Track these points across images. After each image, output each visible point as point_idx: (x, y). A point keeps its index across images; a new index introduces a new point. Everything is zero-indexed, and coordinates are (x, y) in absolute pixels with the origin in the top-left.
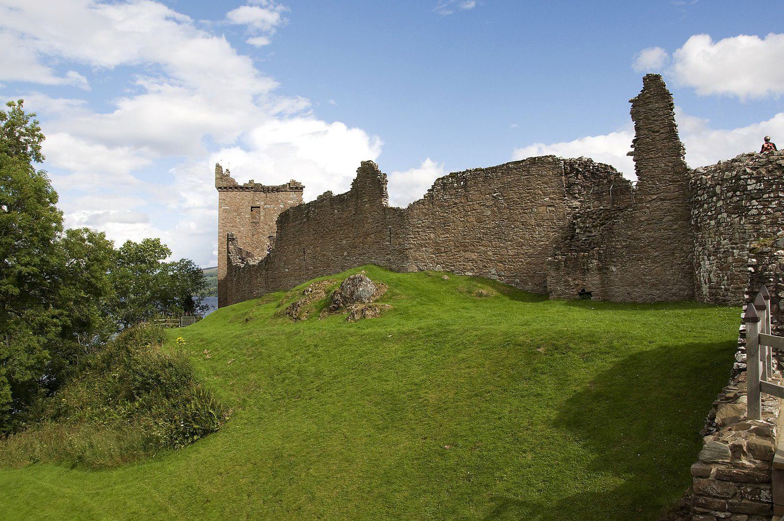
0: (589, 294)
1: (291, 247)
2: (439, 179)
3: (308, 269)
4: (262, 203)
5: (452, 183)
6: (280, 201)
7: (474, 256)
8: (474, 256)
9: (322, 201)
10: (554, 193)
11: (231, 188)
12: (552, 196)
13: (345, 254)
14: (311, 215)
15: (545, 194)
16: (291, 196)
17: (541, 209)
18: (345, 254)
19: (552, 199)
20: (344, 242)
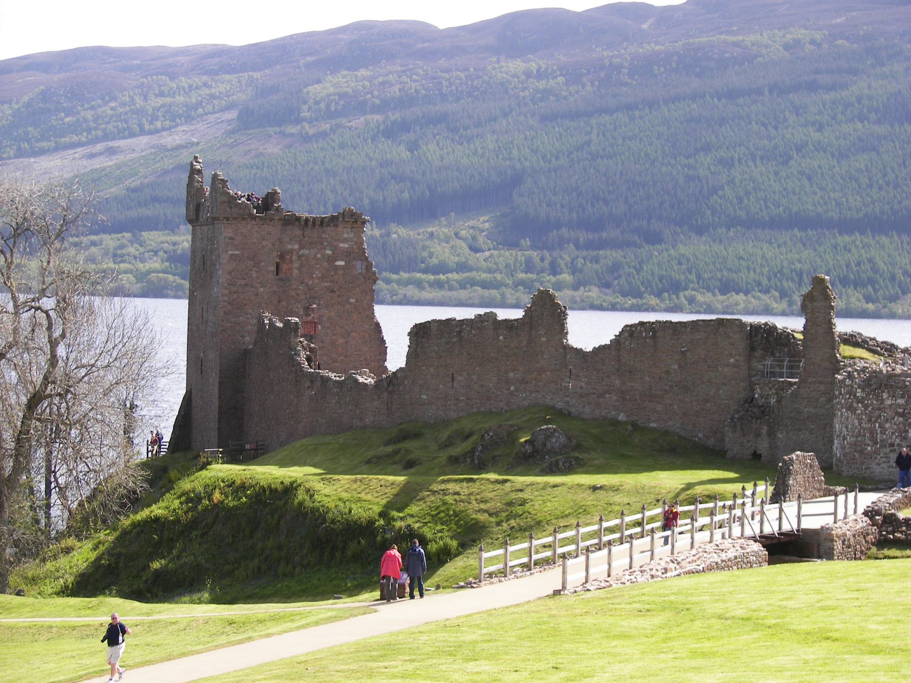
0: (760, 455)
1: (432, 369)
2: (627, 326)
3: (457, 400)
4: (296, 247)
5: (641, 332)
6: (325, 244)
7: (659, 408)
8: (659, 408)
9: (482, 322)
10: (740, 355)
11: (244, 219)
12: (737, 358)
13: (512, 388)
14: (465, 335)
15: (731, 355)
16: (345, 236)
17: (726, 369)
18: (512, 388)
19: (737, 360)
20: (511, 375)
